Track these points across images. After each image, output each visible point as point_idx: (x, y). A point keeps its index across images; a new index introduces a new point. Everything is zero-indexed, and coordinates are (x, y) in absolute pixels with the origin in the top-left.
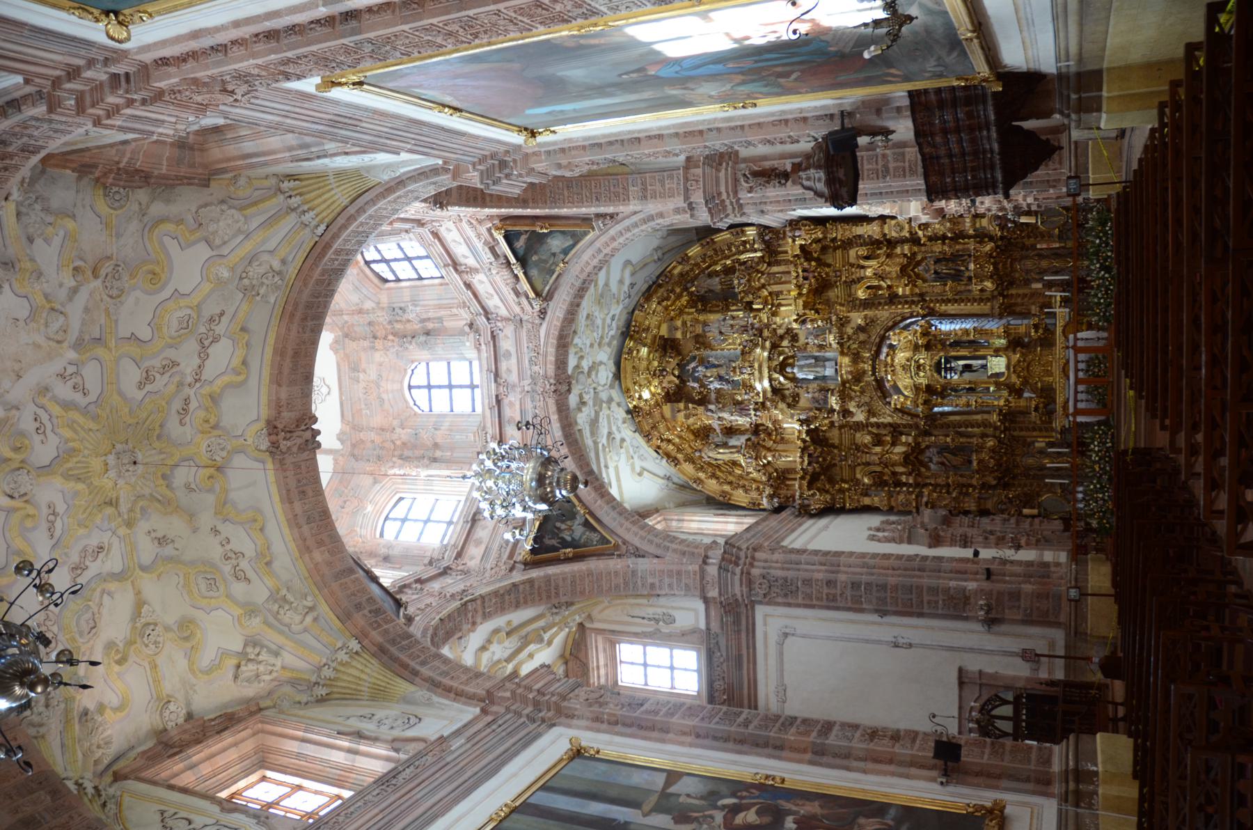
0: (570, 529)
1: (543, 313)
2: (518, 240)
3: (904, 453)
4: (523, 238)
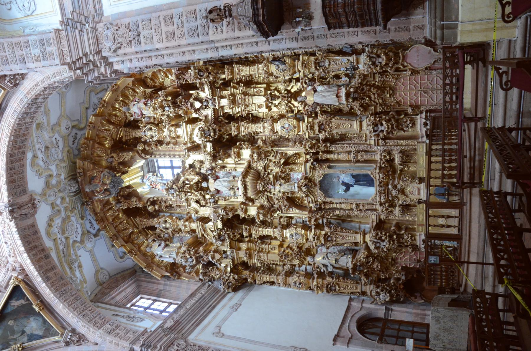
4: (22, 302)
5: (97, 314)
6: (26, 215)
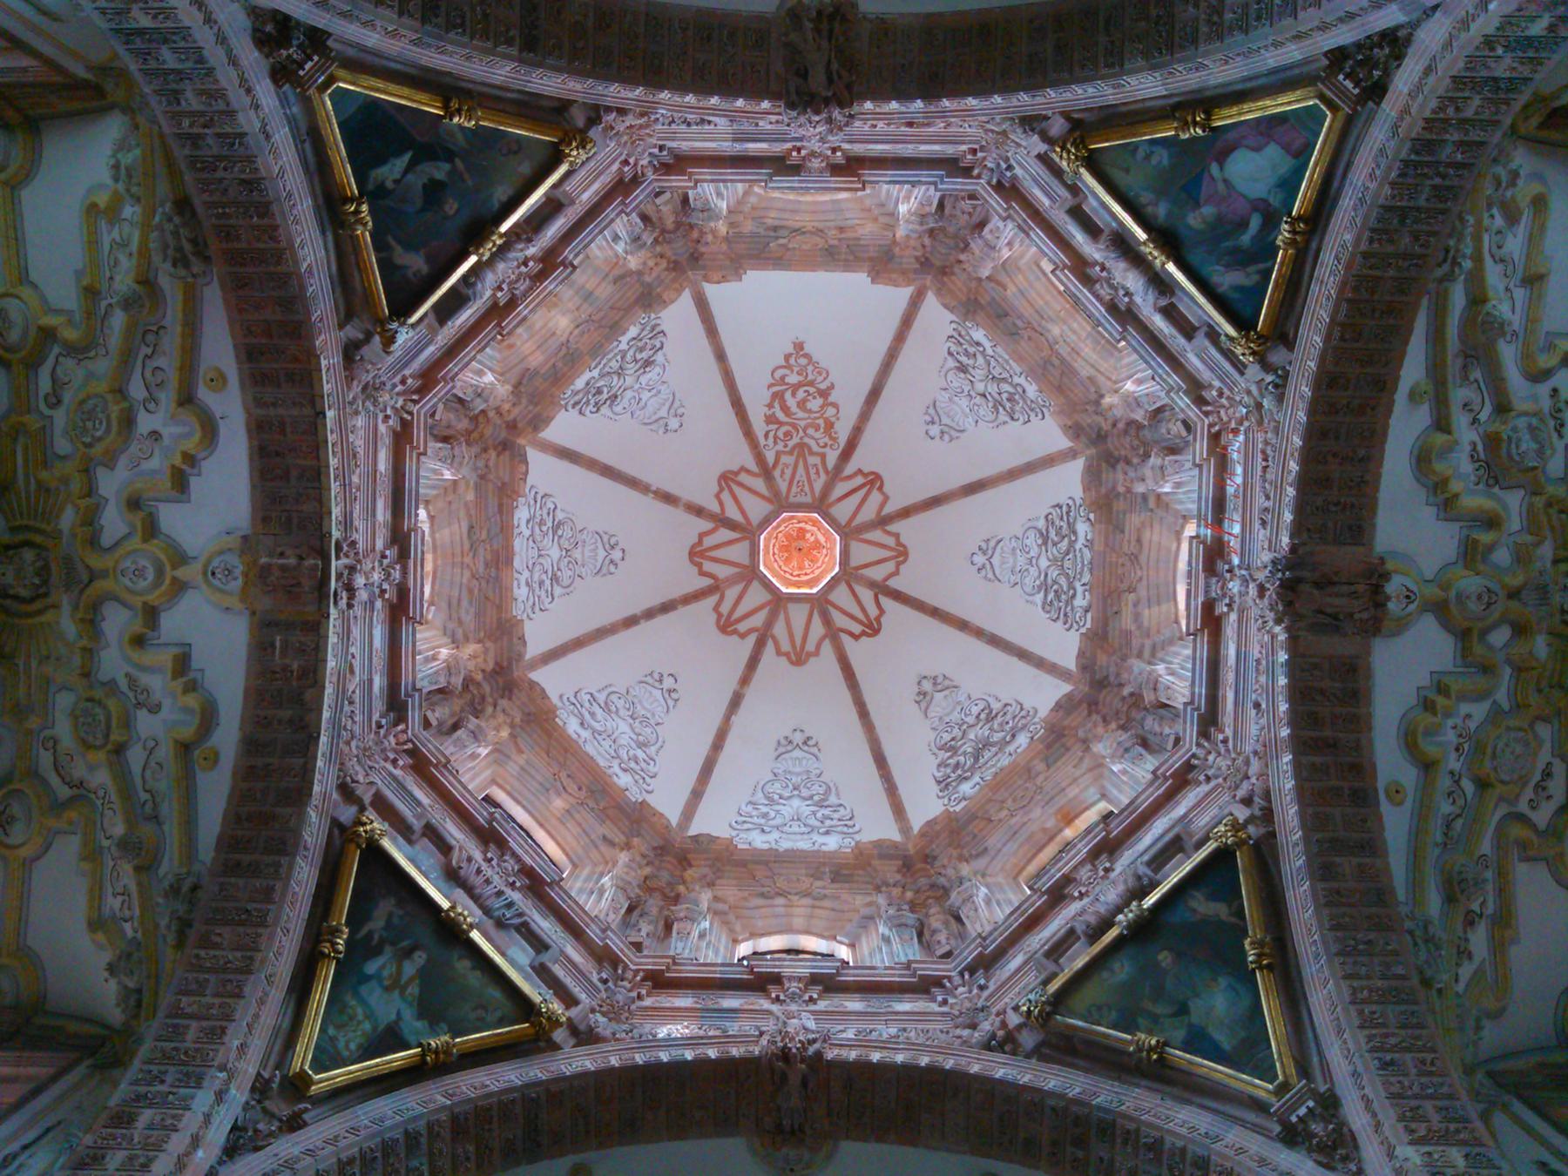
0: (395, 985)
1: (1004, 1043)
2: (1213, 897)
5: (1445, 1090)
6: (1336, 618)
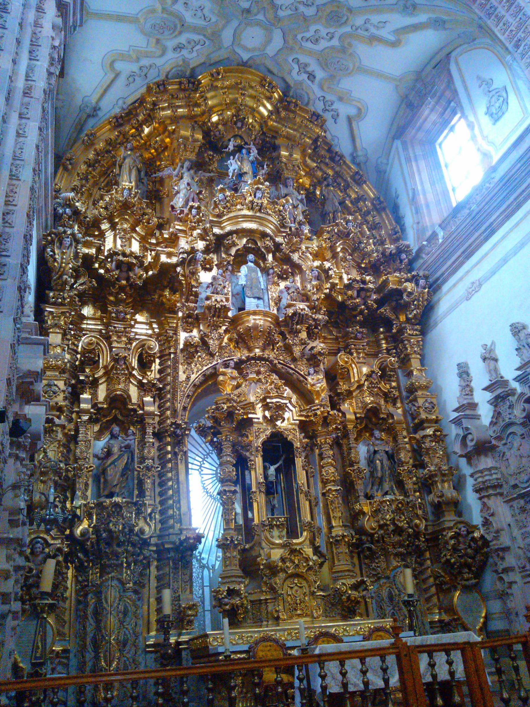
3: (129, 397)
